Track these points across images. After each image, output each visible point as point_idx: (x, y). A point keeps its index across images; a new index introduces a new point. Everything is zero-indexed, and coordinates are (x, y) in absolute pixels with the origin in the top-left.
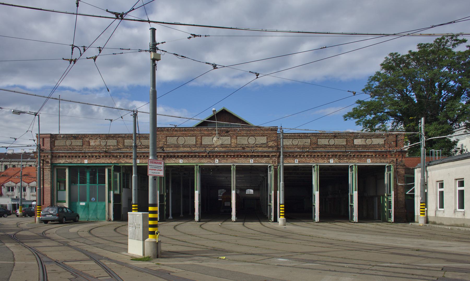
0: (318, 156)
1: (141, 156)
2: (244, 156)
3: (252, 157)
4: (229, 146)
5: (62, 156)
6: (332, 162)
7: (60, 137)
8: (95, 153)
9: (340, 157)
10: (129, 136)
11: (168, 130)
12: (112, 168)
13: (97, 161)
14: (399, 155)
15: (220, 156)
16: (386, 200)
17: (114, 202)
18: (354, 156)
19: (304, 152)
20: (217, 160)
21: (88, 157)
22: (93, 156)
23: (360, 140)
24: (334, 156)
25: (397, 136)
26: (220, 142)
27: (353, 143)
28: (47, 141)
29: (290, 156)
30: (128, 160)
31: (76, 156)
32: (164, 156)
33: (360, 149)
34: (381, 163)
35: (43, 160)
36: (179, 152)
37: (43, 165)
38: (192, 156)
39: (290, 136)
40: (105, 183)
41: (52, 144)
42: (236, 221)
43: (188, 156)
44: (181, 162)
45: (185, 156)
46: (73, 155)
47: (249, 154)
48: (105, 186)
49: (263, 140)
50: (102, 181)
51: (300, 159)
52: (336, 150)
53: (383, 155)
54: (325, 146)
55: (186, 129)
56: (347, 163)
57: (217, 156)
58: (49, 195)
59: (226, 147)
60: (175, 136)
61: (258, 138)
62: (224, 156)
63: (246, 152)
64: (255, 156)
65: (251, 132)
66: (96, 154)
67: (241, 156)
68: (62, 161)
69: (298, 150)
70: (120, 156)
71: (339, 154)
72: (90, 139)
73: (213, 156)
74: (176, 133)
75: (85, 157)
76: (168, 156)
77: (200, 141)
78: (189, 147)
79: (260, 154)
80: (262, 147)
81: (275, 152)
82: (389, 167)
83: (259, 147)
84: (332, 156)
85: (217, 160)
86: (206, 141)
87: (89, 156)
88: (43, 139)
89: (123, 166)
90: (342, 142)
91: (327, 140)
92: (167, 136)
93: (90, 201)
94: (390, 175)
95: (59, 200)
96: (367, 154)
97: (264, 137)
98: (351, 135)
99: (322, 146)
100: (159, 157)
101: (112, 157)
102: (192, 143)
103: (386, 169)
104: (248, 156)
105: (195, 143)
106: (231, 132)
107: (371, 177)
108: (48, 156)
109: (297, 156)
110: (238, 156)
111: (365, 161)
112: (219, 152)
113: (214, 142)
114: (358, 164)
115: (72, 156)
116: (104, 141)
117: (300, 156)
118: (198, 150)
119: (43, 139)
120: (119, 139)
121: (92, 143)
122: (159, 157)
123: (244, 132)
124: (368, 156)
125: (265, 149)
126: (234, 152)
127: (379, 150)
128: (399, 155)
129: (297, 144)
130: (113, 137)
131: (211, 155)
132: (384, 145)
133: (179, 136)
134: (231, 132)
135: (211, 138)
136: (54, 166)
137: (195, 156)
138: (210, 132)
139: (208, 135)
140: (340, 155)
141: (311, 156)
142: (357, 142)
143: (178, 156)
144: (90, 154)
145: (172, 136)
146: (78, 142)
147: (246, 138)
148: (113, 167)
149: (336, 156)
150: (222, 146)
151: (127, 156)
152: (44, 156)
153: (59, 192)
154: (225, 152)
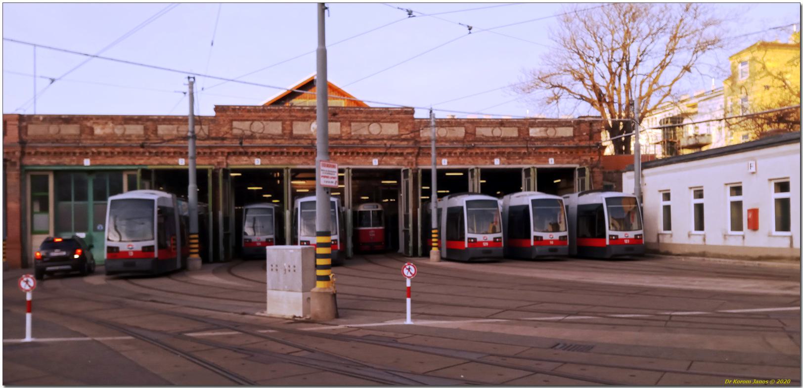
2: (364, 153)
3: (375, 155)
6: (497, 163)
8: (104, 147)
9: (509, 156)
10: (182, 120)
13: (108, 161)
19: (457, 148)
23: (538, 129)
24: (500, 154)
30: (182, 162)
31: (68, 154)
32: (229, 153)
33: (538, 144)
34: (568, 163)
38: (276, 153)
41: (22, 130)
43: (270, 153)
45: (264, 153)
46: (62, 150)
49: (392, 129)
51: (451, 160)
52: (503, 145)
56: (520, 163)
58: (17, 222)
60: (248, 120)
61: (385, 125)
63: (366, 148)
64: (380, 154)
65: (374, 115)
67: (358, 154)
68: (43, 161)
69: (447, 145)
70: (150, 153)
74: (248, 114)
75: (86, 155)
76: (234, 153)
77: (289, 128)
78: (271, 138)
82: (582, 171)
84: (498, 153)
87: (93, 153)
90: (513, 132)
92: (232, 121)
94: (583, 182)
95: (36, 228)
96: (549, 150)
103: (577, 173)
108: (14, 153)
109: (445, 154)
113: (312, 130)
115: (61, 153)
116: (120, 127)
117: (450, 153)
121: (98, 131)
123: (362, 115)
126: (347, 148)
127: (566, 145)
133: (253, 121)
134: (341, 115)
135: (306, 124)
140: (509, 153)
142: (534, 132)
143: (253, 153)
144: (94, 150)
145: (241, 120)
146: (72, 130)
147: (366, 124)
148: (139, 171)
149: (504, 153)
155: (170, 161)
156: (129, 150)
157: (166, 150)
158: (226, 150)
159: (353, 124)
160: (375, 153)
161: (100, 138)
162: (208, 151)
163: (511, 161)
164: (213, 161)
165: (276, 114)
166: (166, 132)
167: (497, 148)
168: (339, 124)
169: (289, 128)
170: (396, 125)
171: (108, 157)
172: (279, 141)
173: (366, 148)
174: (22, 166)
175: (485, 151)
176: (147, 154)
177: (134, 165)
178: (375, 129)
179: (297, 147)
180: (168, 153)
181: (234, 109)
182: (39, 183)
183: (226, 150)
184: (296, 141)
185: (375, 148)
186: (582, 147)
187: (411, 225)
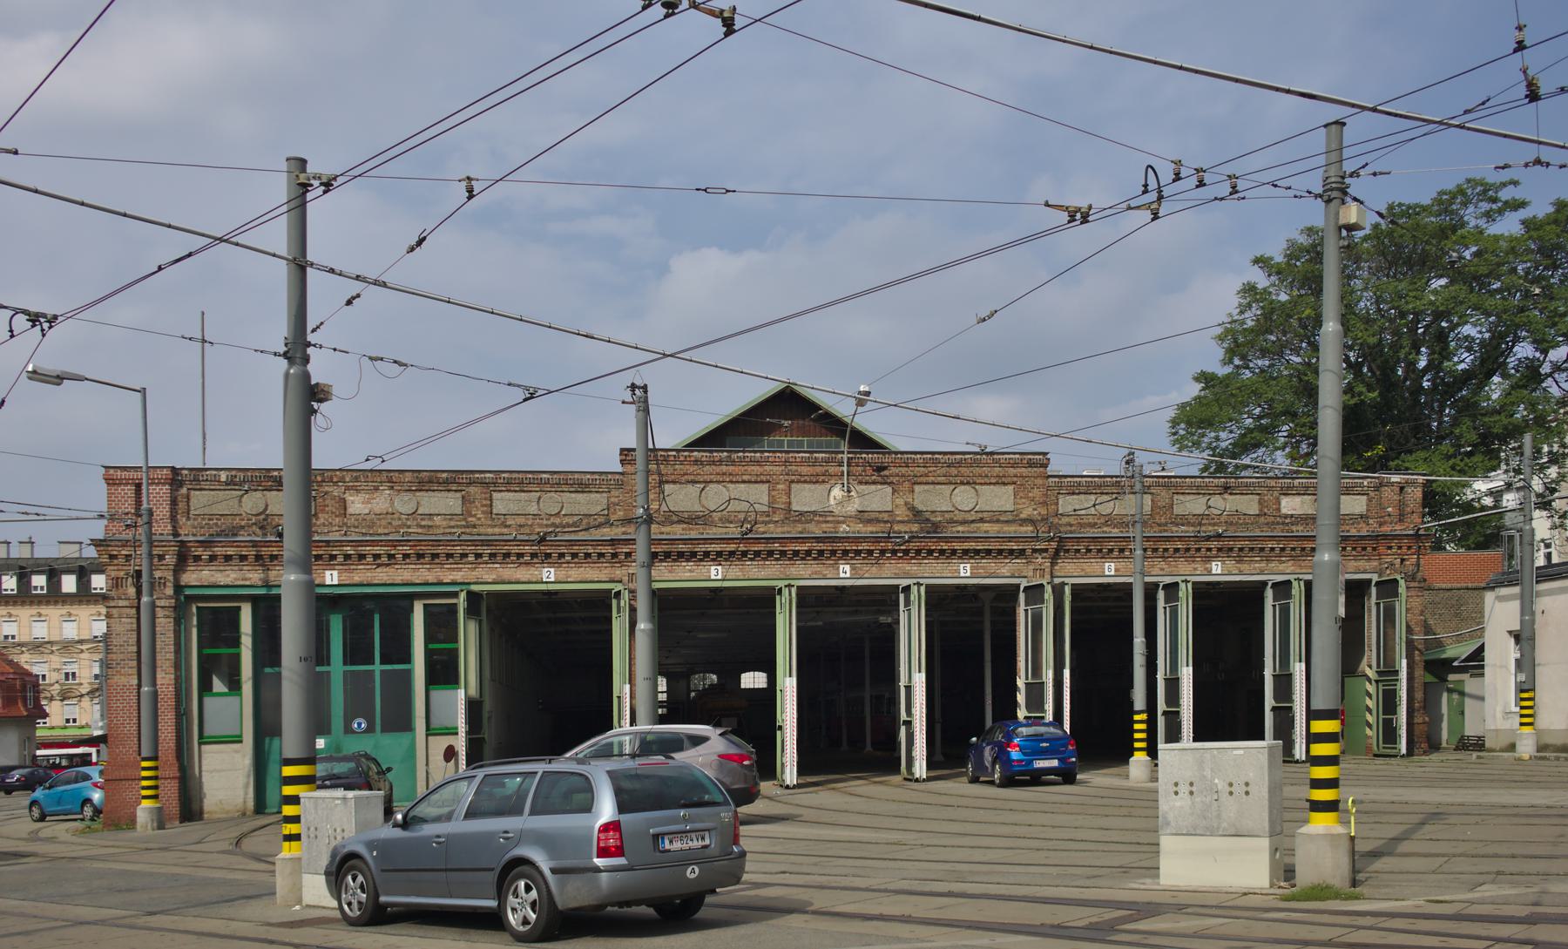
0: (1177, 550)
1: (562, 555)
2: (942, 552)
4: (886, 517)
5: (228, 558)
9: (1240, 555)
14: (1409, 548)
15: (858, 552)
16: (1371, 688)
17: (468, 733)
18: (1283, 549)
20: (847, 568)
21: (340, 559)
22: (362, 557)
23: (1298, 499)
25: (1402, 489)
26: (854, 506)
27: (1279, 509)
28: (158, 498)
29: (1089, 551)
38: (757, 554)
39: (1088, 485)
43: (744, 554)
44: (716, 574)
45: (732, 553)
47: (957, 546)
49: (1000, 498)
50: (398, 650)
51: (1122, 564)
54: (1200, 519)
57: (846, 552)
59: (878, 521)
60: (694, 482)
62: (870, 552)
63: (947, 540)
64: (977, 552)
65: (963, 470)
66: (377, 550)
67: (930, 552)
68: (227, 576)
69: (1115, 532)
71: (1239, 545)
72: (348, 488)
73: (833, 552)
76: (667, 555)
77: (784, 499)
80: (998, 521)
84: (1220, 550)
85: (847, 568)
86: (805, 498)
87: (347, 557)
89: (489, 593)
91: (1203, 500)
93: (348, 730)
98: (1273, 483)
99: (1183, 520)
101: (442, 559)
104: (954, 552)
106: (894, 470)
109: (1111, 551)
110: (918, 552)
112: (857, 540)
113: (832, 502)
116: (406, 496)
117: (1122, 551)
120: (472, 489)
125: (1011, 530)
127: (1353, 532)
128: (1409, 548)
130: (446, 482)
131: (831, 549)
134: (894, 470)
136: (187, 597)
137: (770, 553)
138: (819, 469)
139: (815, 480)
140: (1241, 549)
141: (1155, 550)
143: (707, 554)
147: (947, 489)
149: (1231, 549)
150: (862, 516)
151: (507, 555)
153: (208, 701)
154: (877, 540)
155: (523, 573)
156: (429, 550)
157: (515, 550)
159: (917, 488)
160: (966, 552)
161: (362, 520)
162: (609, 550)
163: (1245, 567)
165: (756, 469)
166: (514, 508)
168: (889, 489)
169: (784, 499)
170: (1011, 488)
171: (379, 566)
173: (947, 540)
174: (178, 588)
176: (471, 558)
178: (964, 498)
179: (803, 540)
180: (520, 555)
182: (219, 625)
184: (800, 527)
186: (1385, 537)
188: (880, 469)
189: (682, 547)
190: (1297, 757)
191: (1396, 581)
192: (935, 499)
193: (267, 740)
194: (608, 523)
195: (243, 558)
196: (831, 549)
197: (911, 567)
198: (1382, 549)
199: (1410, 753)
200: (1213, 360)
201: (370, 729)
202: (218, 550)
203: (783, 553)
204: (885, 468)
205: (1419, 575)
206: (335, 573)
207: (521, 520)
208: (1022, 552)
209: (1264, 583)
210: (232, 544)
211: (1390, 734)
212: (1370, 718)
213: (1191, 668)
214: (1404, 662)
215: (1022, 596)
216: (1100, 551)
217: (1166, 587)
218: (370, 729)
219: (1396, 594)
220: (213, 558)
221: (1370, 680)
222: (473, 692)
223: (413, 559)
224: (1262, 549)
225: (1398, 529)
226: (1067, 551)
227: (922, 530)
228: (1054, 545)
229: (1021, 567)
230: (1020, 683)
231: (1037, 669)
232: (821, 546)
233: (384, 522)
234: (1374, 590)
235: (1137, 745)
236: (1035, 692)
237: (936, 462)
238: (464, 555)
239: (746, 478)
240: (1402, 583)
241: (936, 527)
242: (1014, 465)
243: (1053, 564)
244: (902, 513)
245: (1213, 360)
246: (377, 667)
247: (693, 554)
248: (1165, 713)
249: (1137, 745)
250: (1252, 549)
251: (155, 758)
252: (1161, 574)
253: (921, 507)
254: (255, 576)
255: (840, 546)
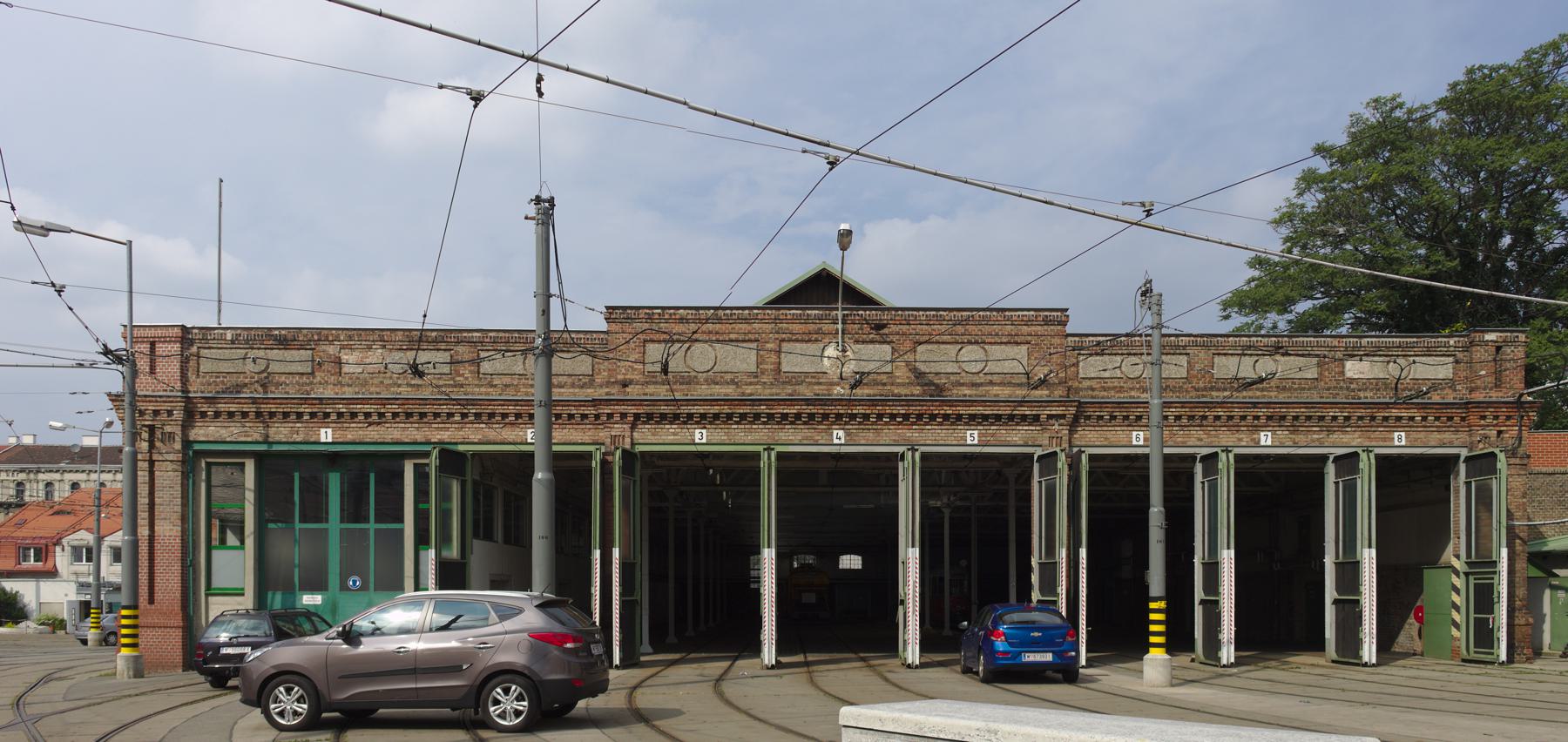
0: (1217, 418)
2: (946, 417)
4: (884, 378)
5: (231, 415)
7: (222, 338)
8: (363, 401)
11: (650, 318)
12: (434, 460)
13: (373, 433)
15: (853, 417)
16: (1459, 582)
18: (1347, 418)
21: (334, 417)
22: (354, 415)
25: (1498, 349)
27: (1343, 373)
29: (1113, 418)
31: (286, 415)
32: (637, 416)
33: (1368, 396)
35: (152, 429)
36: (695, 402)
37: (152, 446)
38: (743, 417)
40: (401, 520)
42: (1239, 662)
43: (729, 416)
45: (716, 416)
47: (962, 410)
48: (402, 530)
49: (1011, 359)
52: (1282, 397)
53: (1463, 412)
55: (721, 313)
57: (839, 416)
61: (997, 351)
62: (866, 417)
63: (951, 403)
64: (985, 417)
66: (367, 408)
67: (933, 417)
73: (825, 416)
77: (773, 358)
78: (733, 382)
79: (1005, 410)
80: (1010, 384)
81: (1060, 403)
83: (999, 384)
84: (1269, 418)
85: (841, 433)
86: (796, 360)
87: (340, 415)
88: (153, 344)
89: (475, 454)
96: (1395, 412)
97: (1016, 349)
98: (1335, 342)
100: (617, 417)
101: (430, 418)
102: (743, 367)
104: (959, 417)
105: (753, 369)
106: (894, 328)
107: (1413, 491)
108: (170, 413)
110: (920, 417)
111: (1384, 440)
114: (1377, 451)
118: (766, 393)
119: (153, 344)
120: (460, 349)
122: (617, 417)
123: (943, 328)
124: (1399, 419)
128: (1509, 418)
129: (1137, 374)
130: (435, 341)
131: (822, 412)
132: (1451, 384)
134: (894, 328)
135: (813, 348)
136: (197, 453)
137: (757, 416)
138: (812, 327)
140: (1296, 418)
143: (690, 416)
146: (295, 360)
148: (435, 453)
149: (1283, 418)
152: (156, 413)
156: (416, 409)
157: (500, 409)
158: (633, 410)
160: (972, 417)
161: (356, 381)
162: (590, 411)
163: (1300, 438)
164: (604, 435)
167: (1268, 404)
168: (887, 348)
170: (1024, 348)
171: (370, 424)
172: (749, 389)
173: (951, 403)
174: (187, 443)
175: (1237, 412)
176: (457, 418)
177: (428, 443)
180: (504, 416)
181: (652, 314)
183: (633, 410)
184: (789, 389)
185: (972, 402)
186: (1478, 404)
187: (1062, 590)
188: (879, 327)
189: (664, 409)
190: (1366, 659)
191: (1493, 455)
192: (939, 360)
193: (270, 595)
194: (591, 384)
195: (245, 415)
196: (822, 412)
197: (913, 434)
198: (1473, 419)
199: (1511, 659)
200: (1273, 244)
201: (364, 588)
202: (222, 407)
203: (770, 417)
204: (884, 326)
205: (1521, 451)
206: (329, 431)
207: (507, 380)
208: (1036, 418)
209: (1324, 458)
210: (232, 401)
211: (1484, 636)
212: (1456, 616)
213: (1232, 552)
214: (1504, 552)
215: (1036, 467)
216: (1126, 418)
217: (1205, 459)
218: (364, 588)
219: (1493, 470)
220: (217, 414)
221: (1457, 573)
222: (453, 552)
223: (402, 418)
224: (1322, 418)
225: (1495, 396)
226: (1088, 418)
227: (924, 392)
228: (1073, 410)
229: (1035, 434)
230: (1034, 562)
231: (1050, 549)
232: (812, 409)
233: (376, 381)
234: (1462, 467)
235: (1153, 639)
236: (1049, 570)
237: (940, 320)
238: (450, 415)
239: (733, 336)
240: (1502, 456)
241: (940, 389)
242: (1028, 323)
243: (1072, 432)
244: (902, 373)
245: (1273, 244)
246: (372, 526)
247: (676, 417)
248: (1202, 602)
249: (1153, 639)
250: (1309, 418)
251: (135, 607)
252: (1194, 442)
253: (922, 367)
254: (254, 432)
255: (833, 409)
